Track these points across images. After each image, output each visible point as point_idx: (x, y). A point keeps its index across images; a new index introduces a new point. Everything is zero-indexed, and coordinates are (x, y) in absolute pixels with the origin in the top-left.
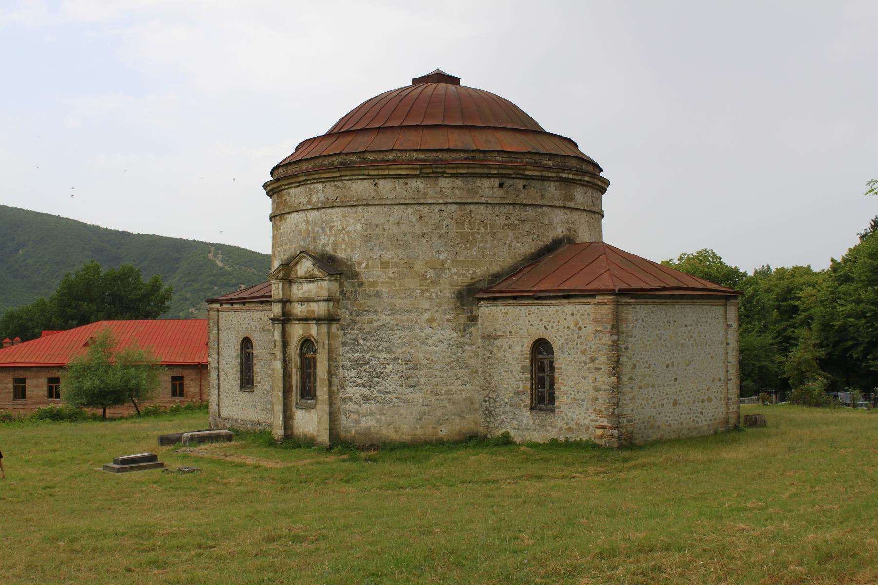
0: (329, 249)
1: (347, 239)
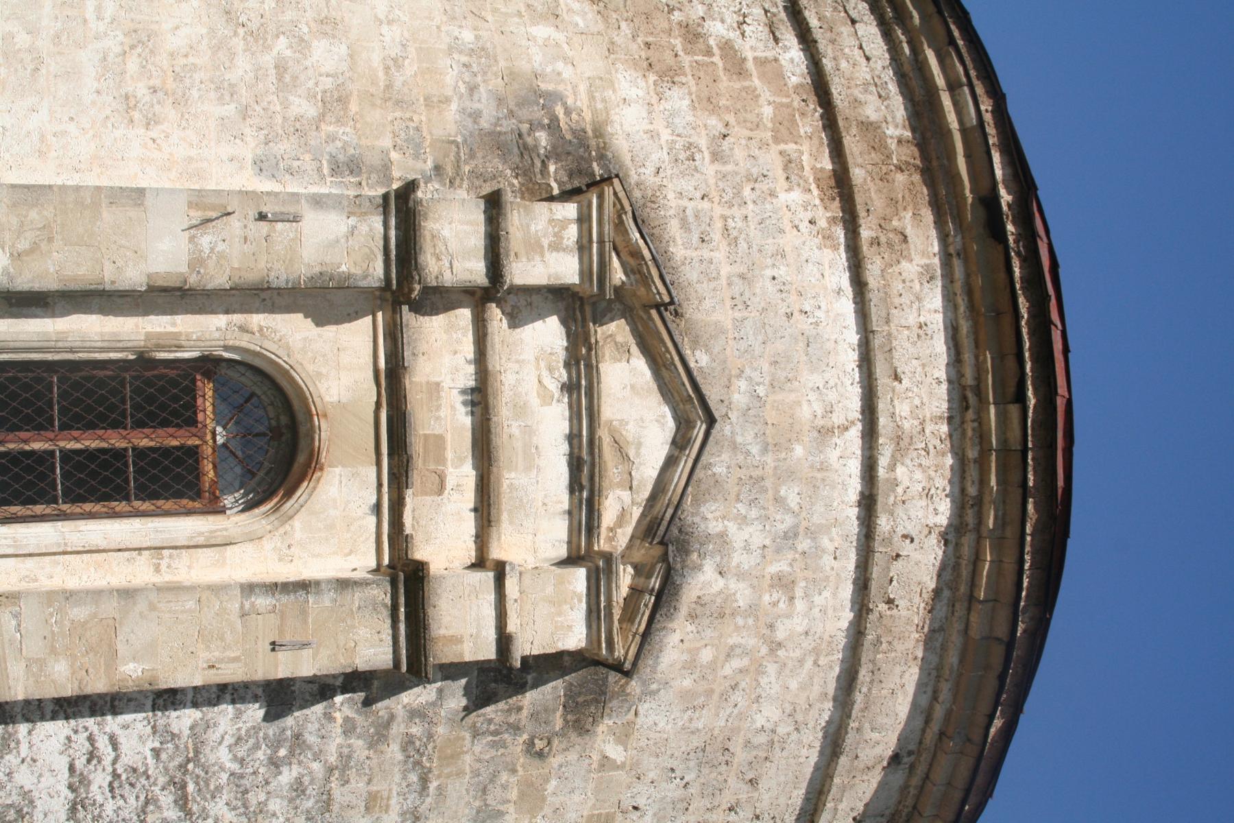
0: (703, 581)
1: (736, 663)
